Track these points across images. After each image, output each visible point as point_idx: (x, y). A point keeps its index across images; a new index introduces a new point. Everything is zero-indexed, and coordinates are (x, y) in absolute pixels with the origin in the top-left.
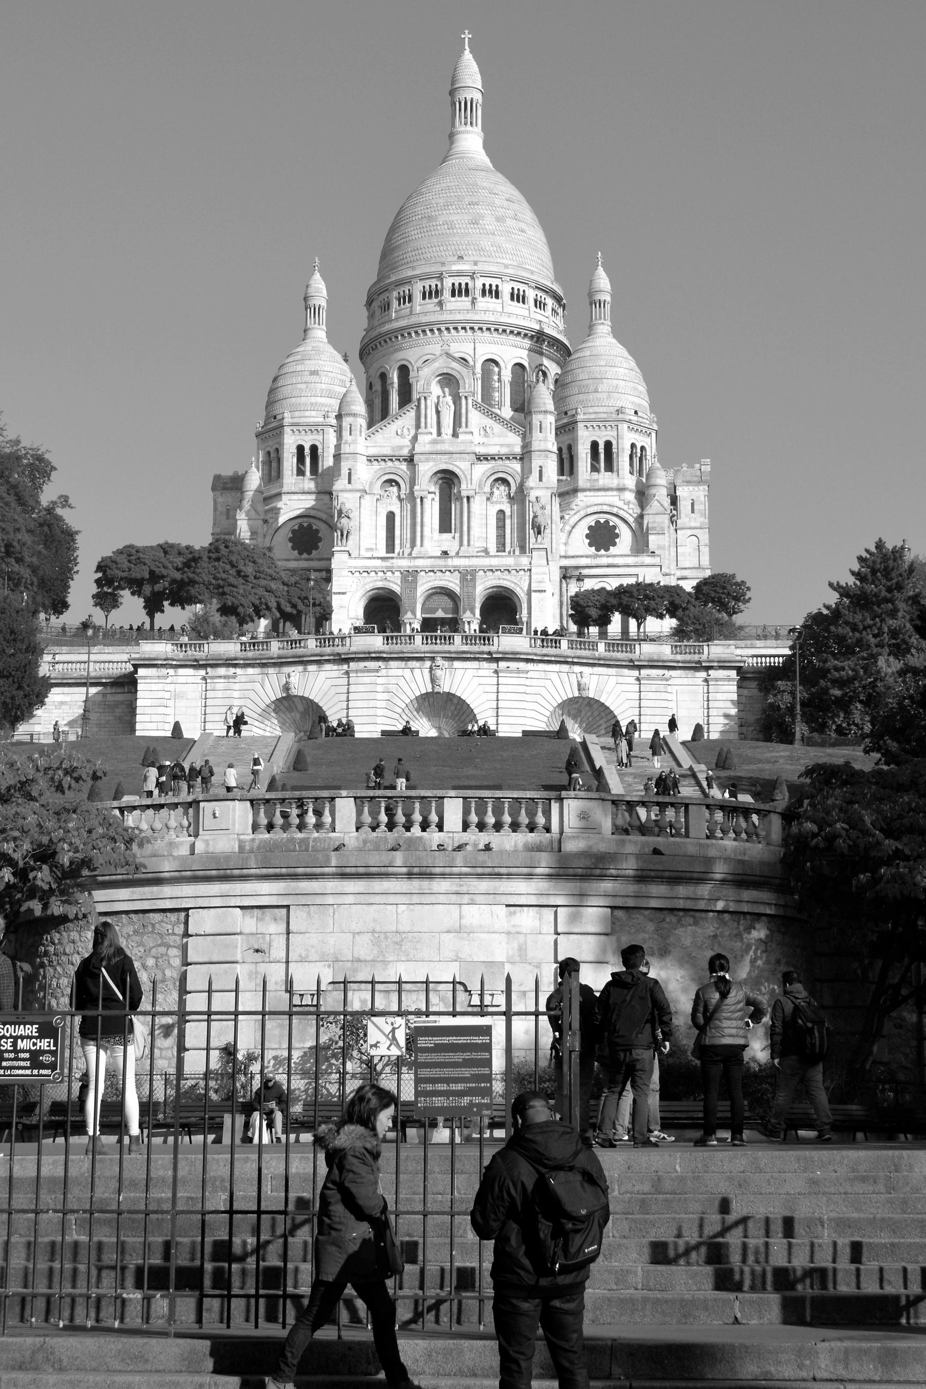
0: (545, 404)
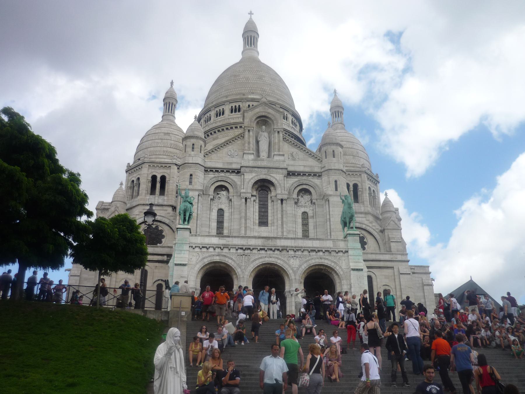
0: (336, 139)
